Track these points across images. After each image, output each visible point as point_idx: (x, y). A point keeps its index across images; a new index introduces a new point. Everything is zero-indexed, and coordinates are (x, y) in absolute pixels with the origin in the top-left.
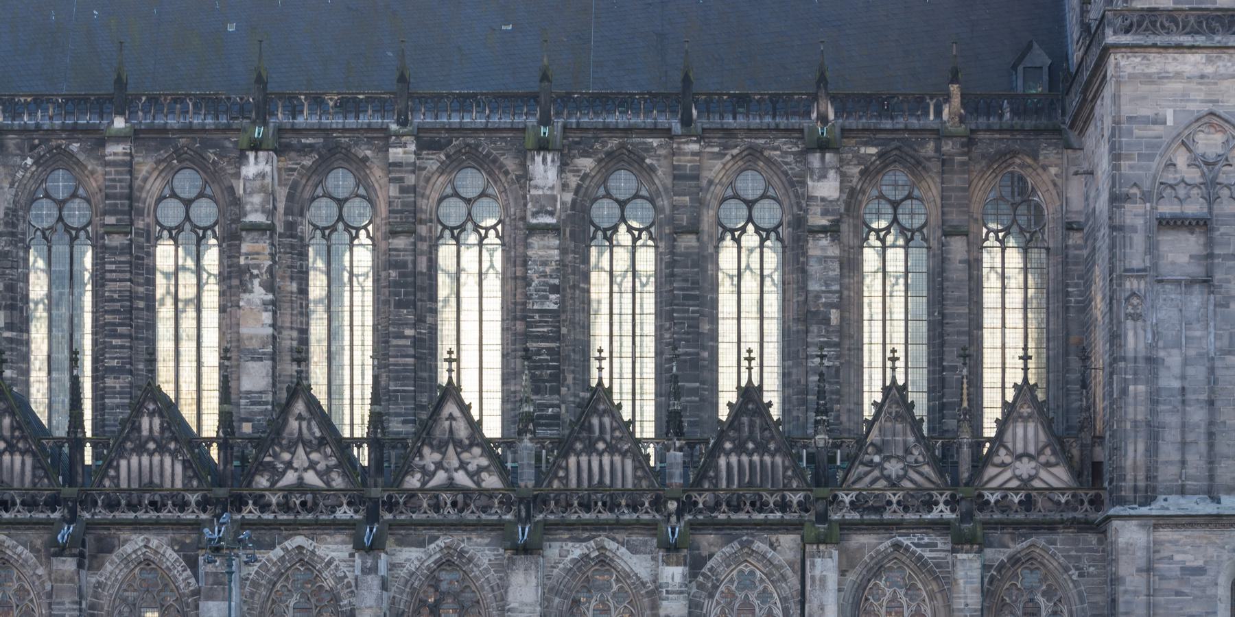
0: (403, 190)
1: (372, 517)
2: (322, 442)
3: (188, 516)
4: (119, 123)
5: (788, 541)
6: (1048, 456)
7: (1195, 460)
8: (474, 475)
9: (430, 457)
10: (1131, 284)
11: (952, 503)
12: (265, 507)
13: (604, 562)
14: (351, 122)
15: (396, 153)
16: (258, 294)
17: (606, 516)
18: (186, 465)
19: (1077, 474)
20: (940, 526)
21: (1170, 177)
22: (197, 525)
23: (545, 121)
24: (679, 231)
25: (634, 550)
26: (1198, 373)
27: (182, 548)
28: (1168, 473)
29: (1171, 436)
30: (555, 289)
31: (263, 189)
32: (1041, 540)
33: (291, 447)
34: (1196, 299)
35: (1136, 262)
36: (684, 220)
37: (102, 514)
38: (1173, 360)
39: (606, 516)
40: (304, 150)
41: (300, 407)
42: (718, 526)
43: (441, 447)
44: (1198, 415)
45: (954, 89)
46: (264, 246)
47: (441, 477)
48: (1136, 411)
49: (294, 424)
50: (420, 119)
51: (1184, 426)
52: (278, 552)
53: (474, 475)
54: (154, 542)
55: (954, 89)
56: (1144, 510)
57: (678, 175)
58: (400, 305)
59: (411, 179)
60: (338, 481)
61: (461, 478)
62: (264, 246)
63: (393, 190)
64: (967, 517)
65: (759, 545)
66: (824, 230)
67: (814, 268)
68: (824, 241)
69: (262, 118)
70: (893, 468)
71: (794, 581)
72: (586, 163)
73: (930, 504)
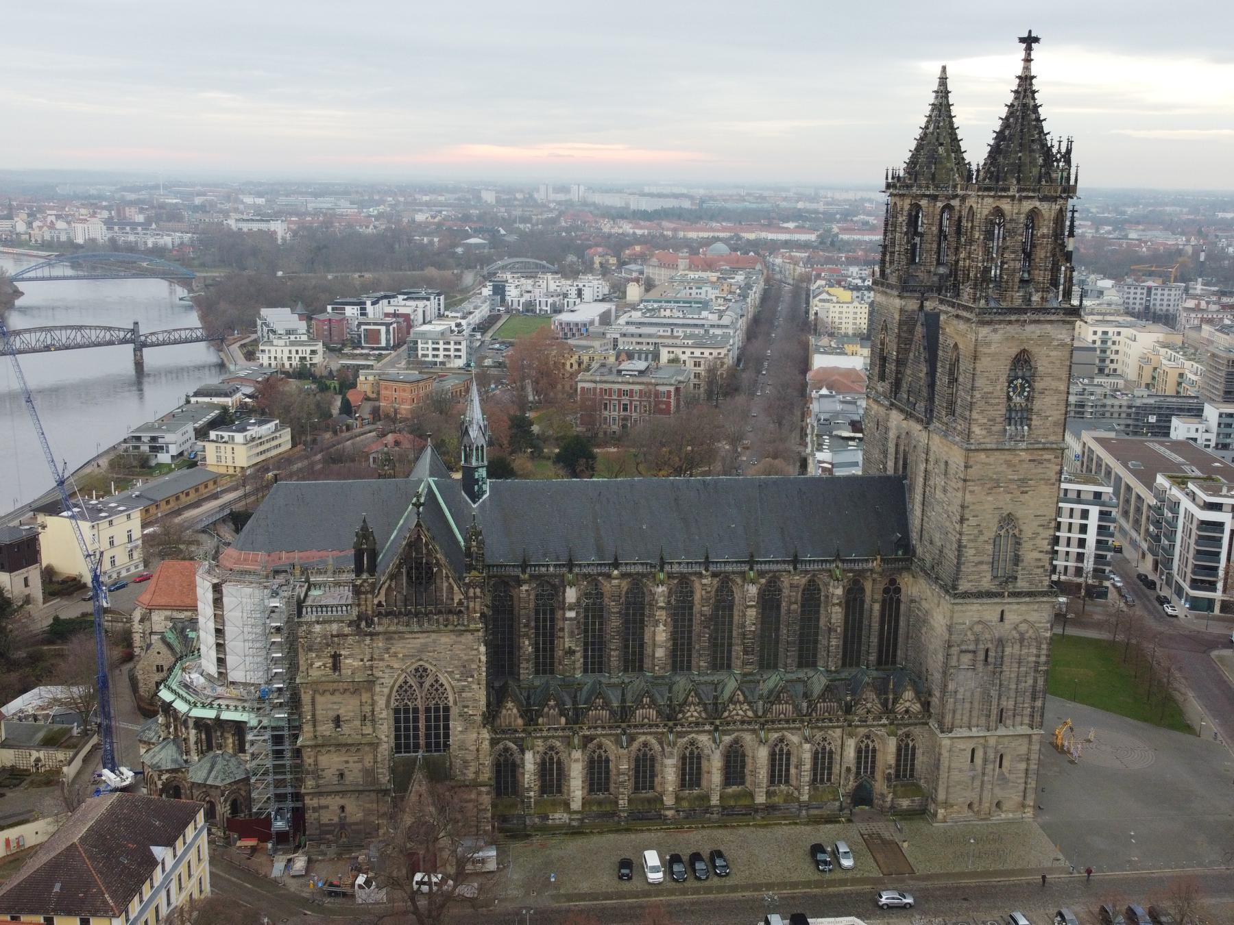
0: (707, 592)
1: (716, 729)
2: (699, 704)
3: (660, 730)
4: (616, 572)
5: (839, 731)
6: (915, 701)
7: (965, 719)
8: (745, 711)
9: (731, 707)
10: (952, 671)
11: (888, 718)
12: (682, 726)
13: (783, 735)
14: (690, 570)
15: (704, 581)
16: (661, 627)
17: (786, 726)
18: (657, 712)
19: (922, 705)
20: (884, 726)
21: (965, 639)
22: (663, 733)
23: (751, 569)
24: (791, 603)
25: (793, 734)
26: (968, 694)
27: (657, 739)
28: (957, 722)
29: (959, 712)
30: (754, 624)
31: (664, 596)
32: (912, 728)
33: (690, 705)
34: (970, 673)
35: (953, 664)
36: (793, 600)
37: (633, 731)
38: (961, 690)
39: (786, 726)
40: (674, 578)
41: (693, 693)
42: (818, 728)
43: (735, 704)
44: (967, 705)
45: (879, 557)
46: (664, 613)
47: (735, 712)
48: (950, 706)
49: (690, 698)
50: (712, 568)
51: (963, 709)
52: (686, 739)
53: (745, 711)
54: (649, 737)
55: (879, 557)
56: (950, 735)
57: (792, 586)
58: (705, 627)
59: (709, 589)
60: (704, 715)
61: (741, 712)
62: (664, 613)
63: (704, 592)
64: (891, 724)
65: (829, 732)
66: (837, 604)
67: (833, 615)
68: (837, 607)
69: (662, 570)
70: (869, 705)
71: (840, 742)
72: (763, 581)
73: (881, 718)
